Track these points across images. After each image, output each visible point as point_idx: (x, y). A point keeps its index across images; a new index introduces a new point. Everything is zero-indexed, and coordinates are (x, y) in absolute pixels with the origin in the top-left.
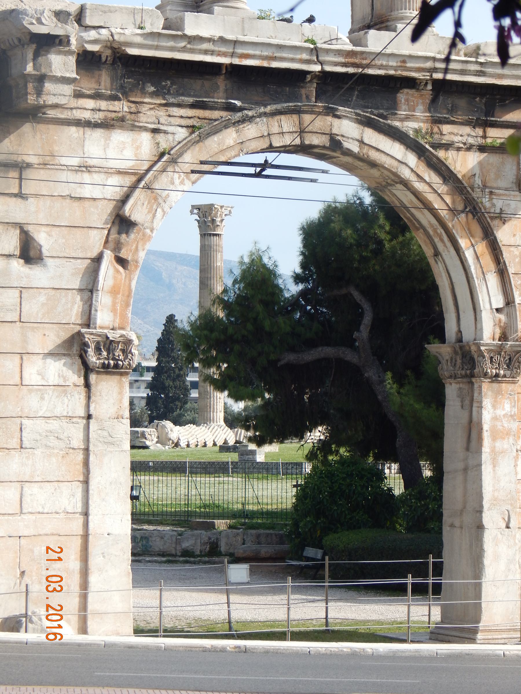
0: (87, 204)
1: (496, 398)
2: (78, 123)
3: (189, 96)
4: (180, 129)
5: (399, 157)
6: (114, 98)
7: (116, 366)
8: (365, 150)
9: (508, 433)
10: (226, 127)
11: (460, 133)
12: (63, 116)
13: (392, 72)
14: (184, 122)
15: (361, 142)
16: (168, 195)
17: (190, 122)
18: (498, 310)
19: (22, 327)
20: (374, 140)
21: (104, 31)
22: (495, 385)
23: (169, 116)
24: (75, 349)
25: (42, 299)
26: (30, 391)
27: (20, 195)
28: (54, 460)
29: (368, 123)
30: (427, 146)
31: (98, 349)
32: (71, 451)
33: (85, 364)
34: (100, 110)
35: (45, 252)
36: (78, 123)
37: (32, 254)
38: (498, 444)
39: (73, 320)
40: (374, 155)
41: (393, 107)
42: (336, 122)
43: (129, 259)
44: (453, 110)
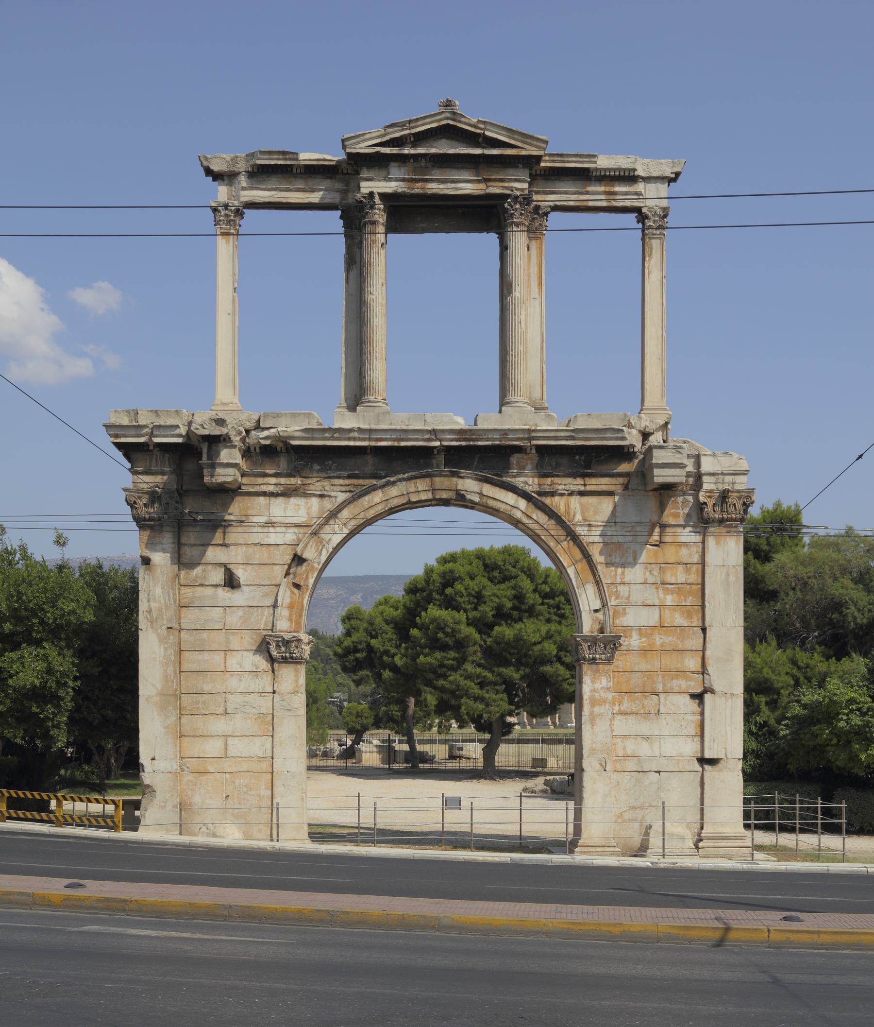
0: (272, 548)
1: (594, 675)
2: (264, 494)
3: (346, 470)
4: (340, 493)
5: (512, 503)
6: (289, 475)
7: (292, 658)
8: (484, 500)
9: (604, 701)
10: (374, 490)
11: (564, 483)
12: (252, 490)
13: (498, 443)
14: (343, 489)
15: (481, 494)
16: (330, 539)
17: (348, 488)
18: (596, 611)
19: (226, 633)
20: (491, 492)
21: (272, 431)
22: (594, 666)
23: (332, 485)
24: (264, 646)
25: (240, 613)
26: (232, 675)
27: (225, 545)
28: (249, 721)
29: (487, 481)
30: (533, 494)
31: (278, 646)
32: (262, 715)
33: (271, 656)
34: (280, 484)
35: (242, 582)
36: (264, 494)
37: (235, 584)
38: (597, 710)
39: (262, 627)
40: (491, 503)
41: (507, 467)
42: (460, 481)
43: (302, 584)
44: (558, 465)
